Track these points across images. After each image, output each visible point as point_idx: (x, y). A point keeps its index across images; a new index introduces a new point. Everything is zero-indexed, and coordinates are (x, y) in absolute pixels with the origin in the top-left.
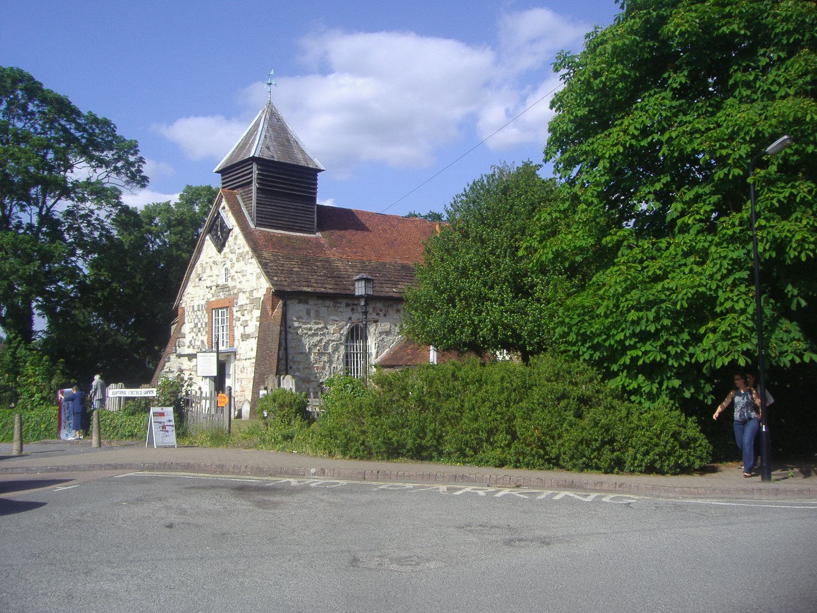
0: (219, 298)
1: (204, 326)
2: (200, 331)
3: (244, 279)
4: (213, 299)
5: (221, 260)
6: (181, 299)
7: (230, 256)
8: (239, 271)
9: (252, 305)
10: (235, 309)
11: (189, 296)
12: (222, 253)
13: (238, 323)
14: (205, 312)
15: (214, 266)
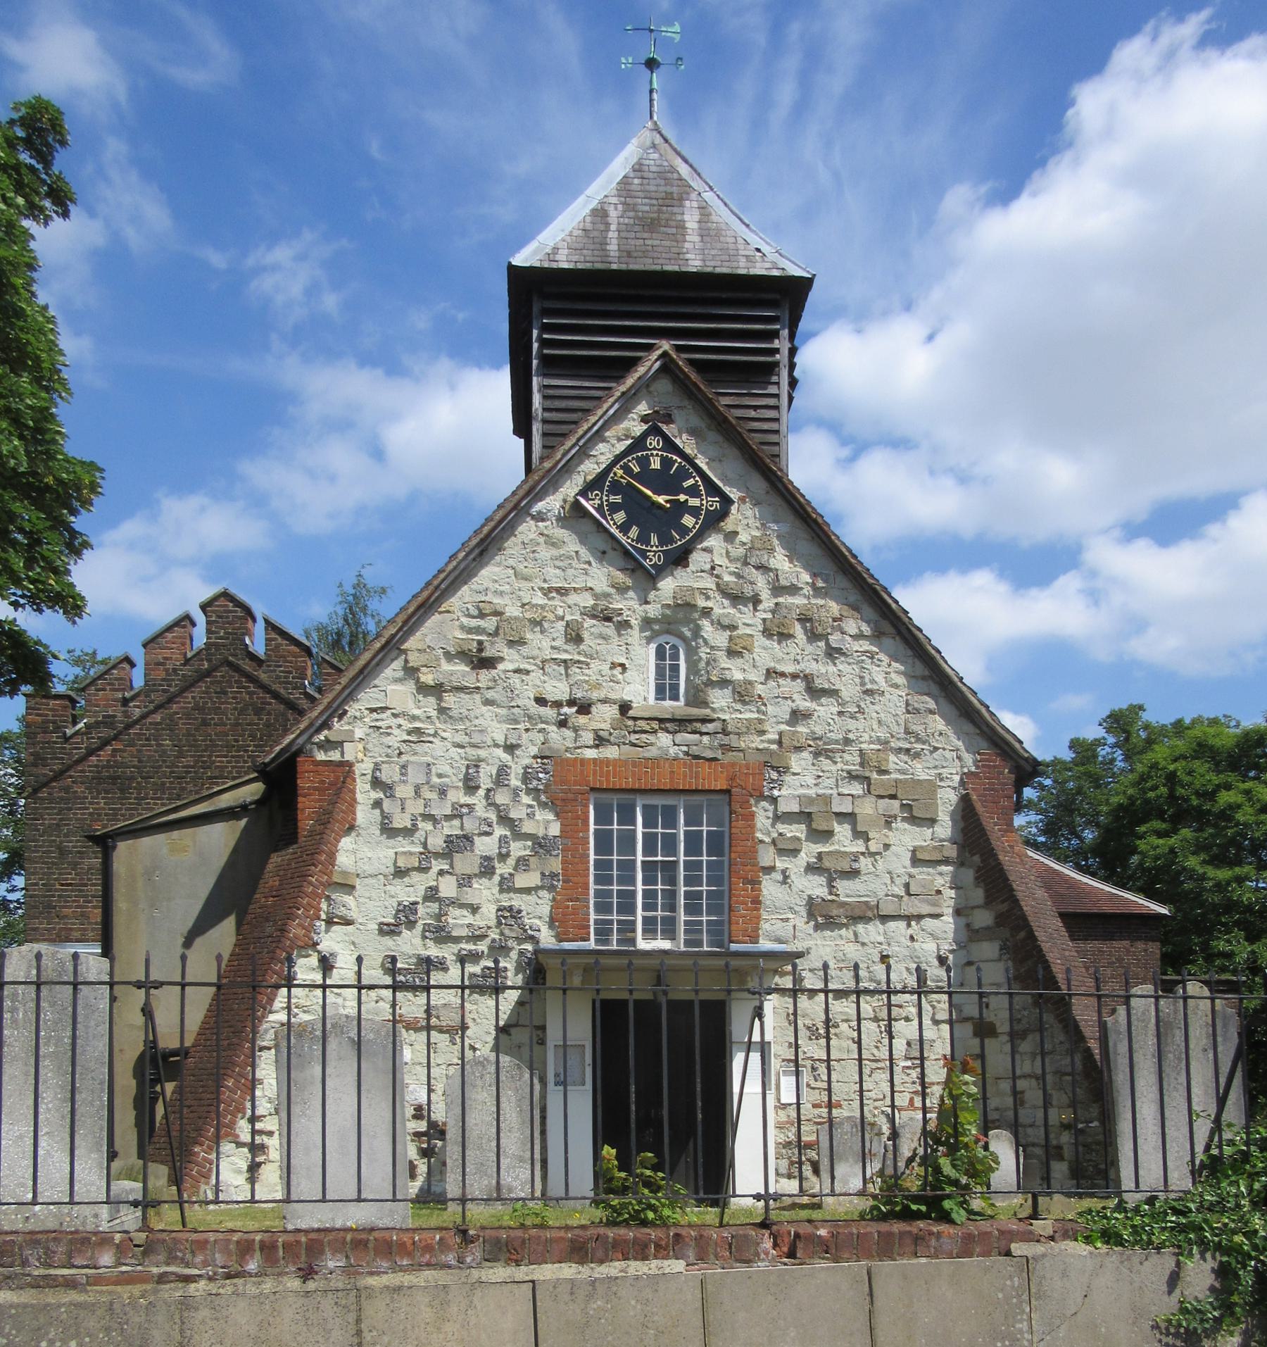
0: (652, 752)
1: (518, 849)
2: (487, 870)
3: (825, 710)
4: (611, 752)
5: (653, 610)
6: (326, 725)
7: (721, 608)
8: (789, 668)
9: (896, 803)
10: (762, 815)
11: (386, 720)
12: (668, 586)
13: (795, 865)
14: (526, 800)
15: (609, 629)
